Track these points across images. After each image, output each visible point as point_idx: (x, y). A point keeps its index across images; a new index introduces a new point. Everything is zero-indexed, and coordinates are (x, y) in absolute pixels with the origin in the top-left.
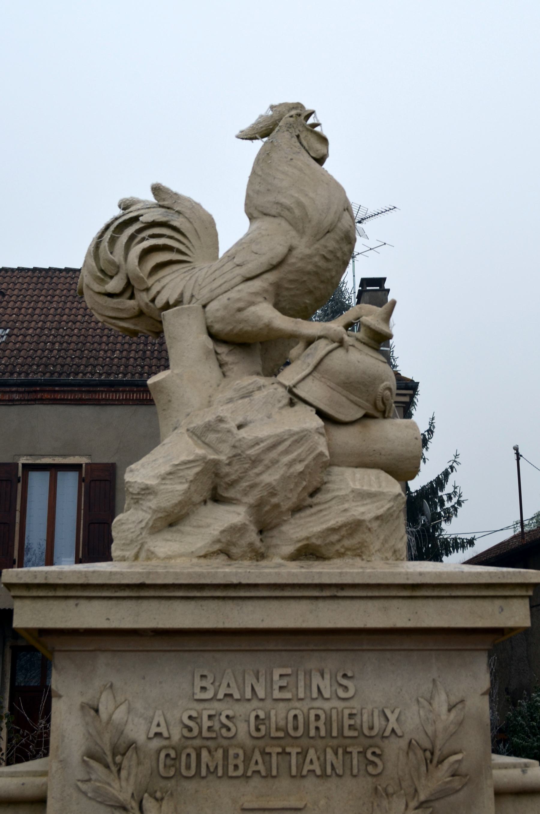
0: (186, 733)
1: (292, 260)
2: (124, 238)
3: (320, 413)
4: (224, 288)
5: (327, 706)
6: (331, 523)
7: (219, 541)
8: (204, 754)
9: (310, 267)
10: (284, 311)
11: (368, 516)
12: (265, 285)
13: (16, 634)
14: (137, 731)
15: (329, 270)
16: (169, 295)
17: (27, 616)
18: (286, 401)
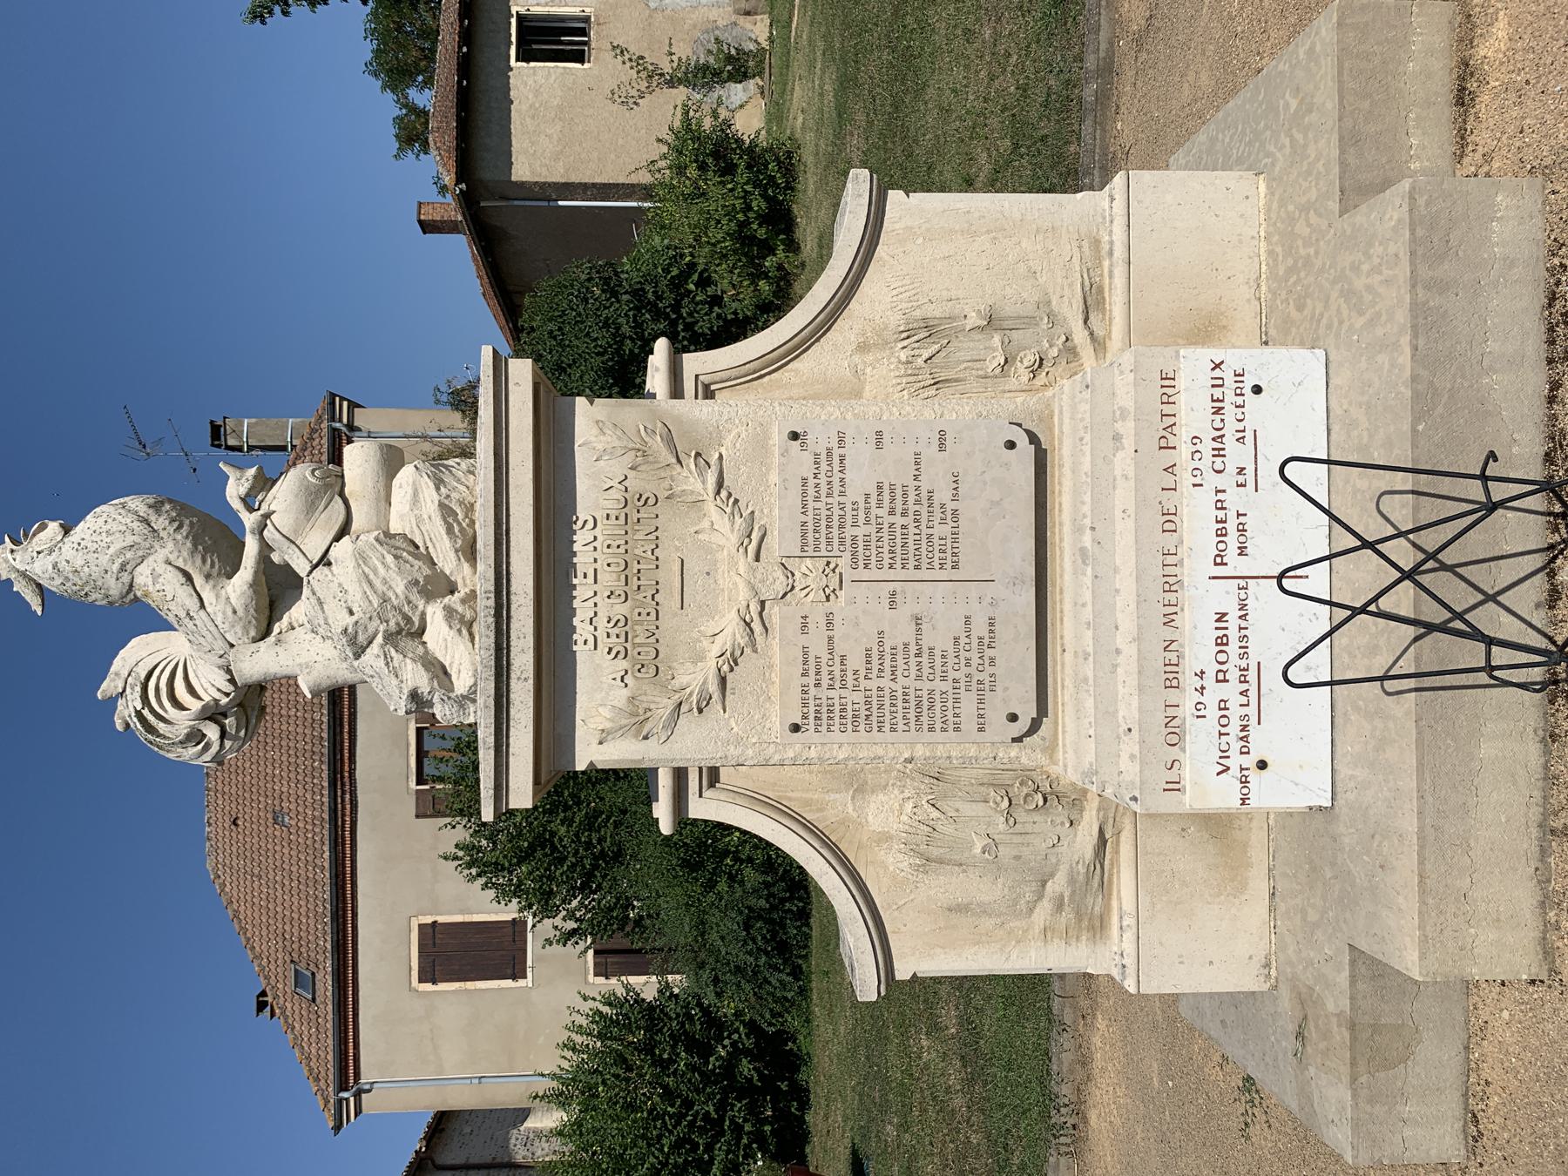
0: (622, 655)
2: (161, 727)
3: (337, 538)
4: (213, 629)
5: (600, 538)
7: (459, 631)
8: (637, 640)
9: (189, 544)
10: (236, 568)
11: (436, 497)
12: (208, 587)
14: (620, 696)
15: (192, 524)
16: (221, 681)
17: (522, 795)
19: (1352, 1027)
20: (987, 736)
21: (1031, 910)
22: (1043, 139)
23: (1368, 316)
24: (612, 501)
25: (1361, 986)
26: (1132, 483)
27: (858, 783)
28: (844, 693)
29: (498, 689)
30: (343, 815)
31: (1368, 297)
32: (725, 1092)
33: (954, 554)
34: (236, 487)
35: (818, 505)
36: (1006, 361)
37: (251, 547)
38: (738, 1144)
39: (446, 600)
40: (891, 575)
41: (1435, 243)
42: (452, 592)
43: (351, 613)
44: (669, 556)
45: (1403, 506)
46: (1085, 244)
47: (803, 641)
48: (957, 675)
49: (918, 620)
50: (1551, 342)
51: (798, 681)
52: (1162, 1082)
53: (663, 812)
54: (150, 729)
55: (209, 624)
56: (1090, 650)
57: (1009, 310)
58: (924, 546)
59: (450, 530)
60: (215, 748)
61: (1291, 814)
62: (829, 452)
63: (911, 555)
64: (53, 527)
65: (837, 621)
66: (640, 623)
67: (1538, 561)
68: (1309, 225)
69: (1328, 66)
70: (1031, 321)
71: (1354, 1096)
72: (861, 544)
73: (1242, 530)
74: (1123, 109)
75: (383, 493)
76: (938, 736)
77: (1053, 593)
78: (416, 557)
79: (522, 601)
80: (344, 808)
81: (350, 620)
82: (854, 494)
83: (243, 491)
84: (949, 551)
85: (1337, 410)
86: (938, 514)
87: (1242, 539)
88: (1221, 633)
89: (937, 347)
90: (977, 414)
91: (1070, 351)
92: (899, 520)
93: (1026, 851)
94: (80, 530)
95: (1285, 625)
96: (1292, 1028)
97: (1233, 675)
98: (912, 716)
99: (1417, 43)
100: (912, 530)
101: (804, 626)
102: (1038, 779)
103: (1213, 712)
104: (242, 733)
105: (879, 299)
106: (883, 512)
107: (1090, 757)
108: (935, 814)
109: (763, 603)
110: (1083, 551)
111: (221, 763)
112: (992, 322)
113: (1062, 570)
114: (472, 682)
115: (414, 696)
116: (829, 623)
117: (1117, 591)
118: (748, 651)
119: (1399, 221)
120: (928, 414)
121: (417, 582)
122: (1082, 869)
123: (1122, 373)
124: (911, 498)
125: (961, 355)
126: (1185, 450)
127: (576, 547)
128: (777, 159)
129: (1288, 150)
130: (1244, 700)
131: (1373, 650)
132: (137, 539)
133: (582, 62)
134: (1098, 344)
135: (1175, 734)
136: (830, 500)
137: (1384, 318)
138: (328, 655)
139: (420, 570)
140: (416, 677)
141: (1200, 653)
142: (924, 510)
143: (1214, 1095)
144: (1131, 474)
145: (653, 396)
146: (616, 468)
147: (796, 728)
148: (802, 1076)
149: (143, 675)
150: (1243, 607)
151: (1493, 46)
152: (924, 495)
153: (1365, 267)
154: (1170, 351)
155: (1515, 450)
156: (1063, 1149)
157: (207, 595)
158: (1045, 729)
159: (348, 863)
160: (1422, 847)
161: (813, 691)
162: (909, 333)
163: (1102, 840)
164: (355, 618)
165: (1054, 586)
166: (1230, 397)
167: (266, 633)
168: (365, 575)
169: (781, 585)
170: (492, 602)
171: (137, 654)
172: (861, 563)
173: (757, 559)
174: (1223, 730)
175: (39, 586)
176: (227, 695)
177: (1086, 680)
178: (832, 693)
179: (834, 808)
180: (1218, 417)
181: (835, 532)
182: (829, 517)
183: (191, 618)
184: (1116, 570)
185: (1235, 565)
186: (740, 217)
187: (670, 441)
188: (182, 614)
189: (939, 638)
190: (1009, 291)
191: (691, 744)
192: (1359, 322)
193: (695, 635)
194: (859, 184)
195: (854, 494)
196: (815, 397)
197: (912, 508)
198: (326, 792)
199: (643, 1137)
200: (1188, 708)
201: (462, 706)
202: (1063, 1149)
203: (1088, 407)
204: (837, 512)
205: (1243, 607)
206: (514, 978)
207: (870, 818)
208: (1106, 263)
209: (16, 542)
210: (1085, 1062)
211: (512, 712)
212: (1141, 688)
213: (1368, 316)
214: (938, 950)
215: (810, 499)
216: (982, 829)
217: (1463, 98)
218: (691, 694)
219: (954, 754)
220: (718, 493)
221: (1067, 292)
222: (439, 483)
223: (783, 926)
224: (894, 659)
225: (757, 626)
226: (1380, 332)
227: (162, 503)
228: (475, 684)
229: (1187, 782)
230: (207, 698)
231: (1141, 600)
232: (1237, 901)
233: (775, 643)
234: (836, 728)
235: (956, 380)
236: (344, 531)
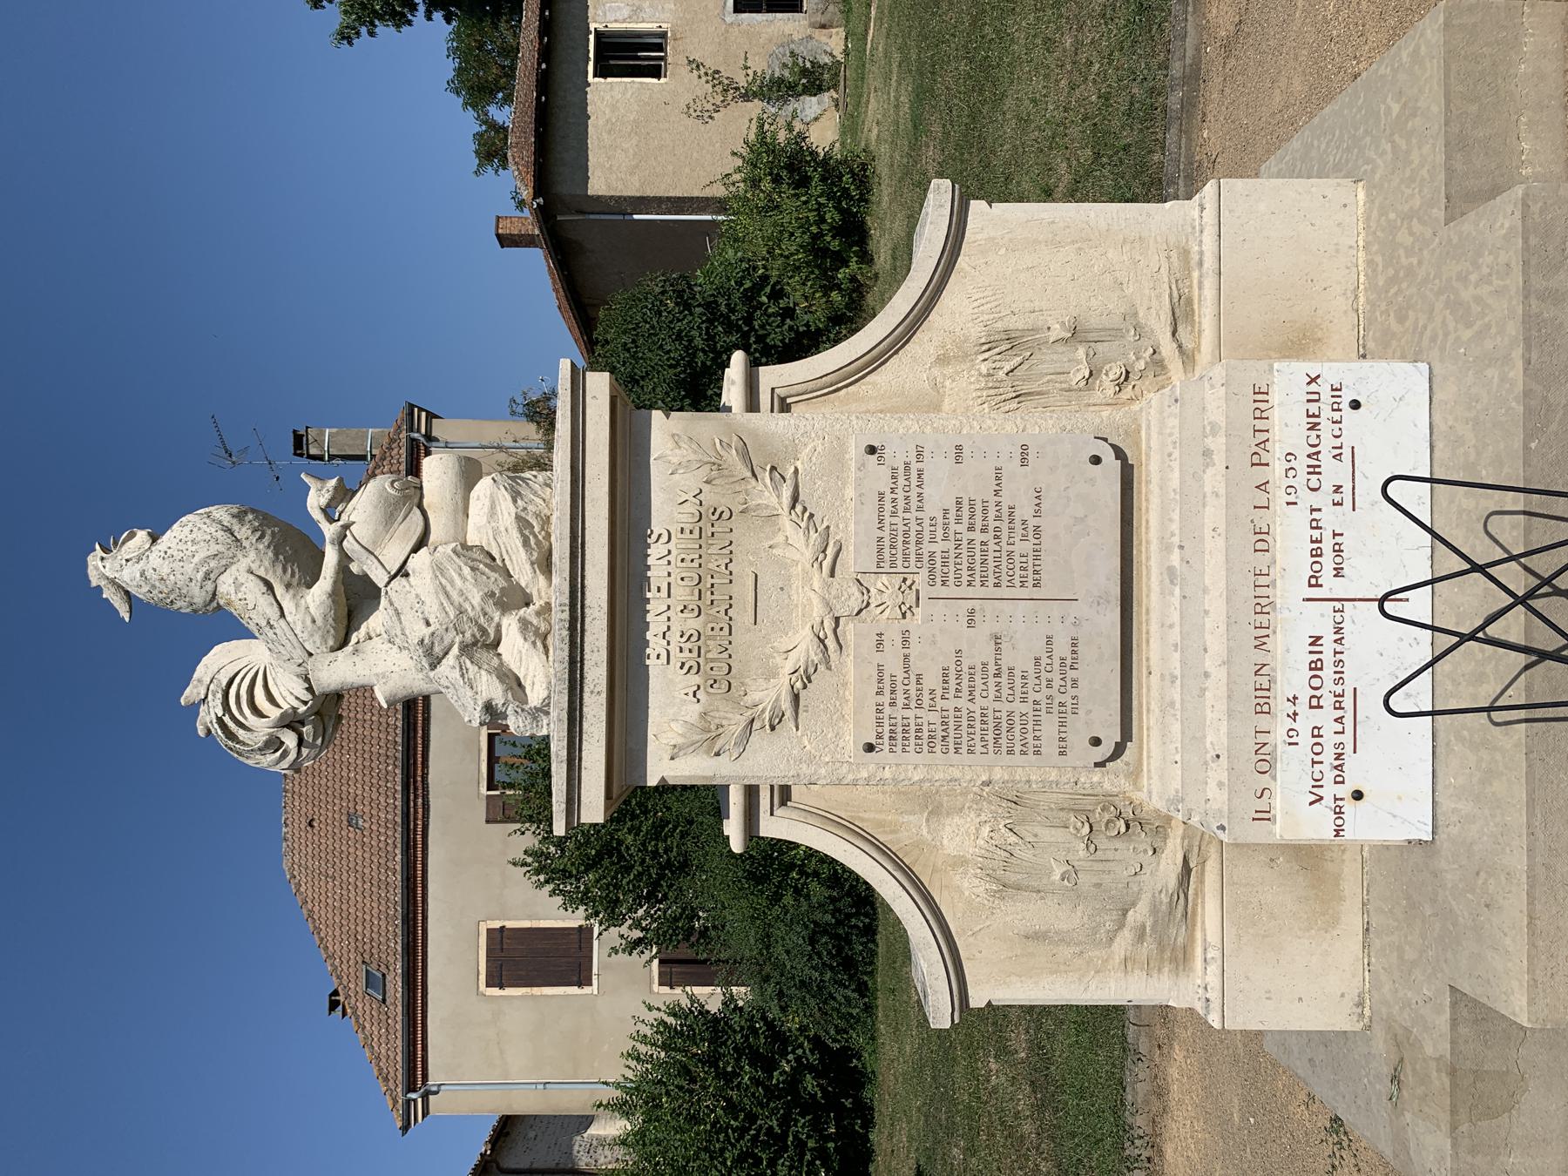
0: (695, 670)
1: (262, 573)
3: (415, 550)
4: (292, 638)
5: (674, 552)
7: (534, 643)
8: (710, 655)
9: (270, 554)
10: (315, 578)
11: (513, 510)
12: (289, 596)
13: (611, 820)
14: (692, 711)
15: (273, 533)
17: (594, 811)
18: (403, 580)
19: (1453, 1072)
22: (1126, 148)
23: (1476, 328)
25: (1463, 1030)
26: (1223, 501)
27: (933, 805)
28: (919, 712)
30: (416, 819)
31: (1476, 309)
32: (789, 1107)
33: (1036, 572)
34: (317, 498)
35: (894, 520)
36: (1091, 374)
37: (331, 558)
38: (801, 1160)
42: (527, 605)
43: (428, 624)
44: (743, 570)
45: (1513, 527)
46: (1174, 254)
48: (1038, 697)
49: (997, 639)
52: (1244, 1119)
53: (733, 830)
54: (231, 735)
55: (289, 633)
56: (1178, 672)
57: (1094, 321)
58: (1004, 563)
59: (526, 543)
60: (292, 756)
61: (1387, 847)
62: (907, 466)
63: (990, 573)
64: (142, 536)
65: (913, 639)
66: (713, 638)
68: (1411, 234)
69: (1432, 70)
70: (1116, 333)
71: (1454, 1145)
72: (939, 560)
73: (1338, 551)
74: (1210, 117)
75: (460, 505)
76: (1017, 758)
77: (1139, 614)
79: (597, 614)
80: (416, 812)
81: (427, 631)
82: (932, 509)
83: (323, 501)
84: (1031, 569)
85: (1441, 426)
87: (1338, 560)
89: (1019, 359)
91: (1157, 364)
92: (978, 536)
93: (1107, 879)
94: (167, 539)
95: (1385, 652)
96: (1386, 1071)
97: (1328, 701)
98: (990, 737)
99: (1529, 44)
100: (992, 546)
101: (880, 643)
102: (1120, 805)
103: (1305, 740)
104: (319, 741)
105: (959, 310)
106: (962, 528)
107: (1176, 784)
108: (1013, 839)
109: (837, 620)
110: (1171, 571)
111: (298, 771)
112: (1076, 334)
113: (1148, 587)
114: (545, 694)
115: (489, 707)
116: (905, 641)
117: (1206, 612)
118: (821, 668)
119: (1511, 228)
120: (1009, 428)
121: (492, 594)
122: (1166, 900)
123: (1212, 387)
124: (992, 514)
125: (1044, 368)
126: (1279, 467)
127: (650, 561)
128: (852, 171)
129: (1389, 156)
130: (1339, 728)
131: (1480, 678)
132: (220, 548)
133: (659, 77)
134: (1187, 357)
135: (1265, 762)
136: (907, 515)
137: (1493, 330)
138: (405, 666)
139: (496, 582)
140: (490, 688)
141: (1292, 678)
142: (1005, 527)
143: (1300, 1134)
144: (1222, 491)
145: (729, 409)
146: (690, 481)
147: (870, 748)
148: (867, 1094)
150: (1338, 630)
152: (1005, 511)
153: (1473, 278)
154: (1263, 364)
157: (288, 605)
158: (1128, 754)
159: (419, 866)
160: (1531, 886)
161: (887, 710)
162: (990, 345)
163: (1186, 869)
164: (431, 629)
165: (1140, 605)
166: (1327, 413)
167: (343, 643)
168: (441, 587)
169: (855, 602)
170: (566, 615)
171: (219, 661)
172: (938, 580)
173: (832, 574)
174: (1317, 758)
175: (127, 593)
176: (305, 703)
177: (1172, 704)
178: (907, 713)
179: (907, 832)
180: (1314, 433)
181: (913, 548)
182: (906, 533)
183: (272, 627)
184: (1205, 591)
185: (1331, 586)
186: (814, 229)
187: (745, 454)
188: (263, 623)
189: (1019, 658)
191: (764, 762)
192: (1467, 334)
193: (768, 650)
194: (940, 194)
195: (932, 509)
196: (893, 410)
197: (992, 524)
198: (399, 796)
199: (706, 1149)
200: (1279, 735)
201: (535, 718)
203: (1176, 422)
204: (914, 527)
205: (1338, 630)
206: (580, 985)
207: (945, 842)
208: (1196, 274)
209: (106, 550)
210: (1160, 1093)
212: (1230, 714)
213: (1476, 328)
214: (1014, 978)
215: (887, 514)
216: (1062, 856)
218: (763, 711)
219: (1033, 778)
220: (793, 507)
221: (1154, 303)
222: (516, 495)
223: (849, 942)
224: (971, 679)
226: (1489, 344)
227: (246, 513)
228: (549, 697)
229: (1278, 811)
230: (286, 706)
231: (1231, 623)
232: (1328, 936)
233: (850, 661)
234: (911, 748)
235: (1039, 393)
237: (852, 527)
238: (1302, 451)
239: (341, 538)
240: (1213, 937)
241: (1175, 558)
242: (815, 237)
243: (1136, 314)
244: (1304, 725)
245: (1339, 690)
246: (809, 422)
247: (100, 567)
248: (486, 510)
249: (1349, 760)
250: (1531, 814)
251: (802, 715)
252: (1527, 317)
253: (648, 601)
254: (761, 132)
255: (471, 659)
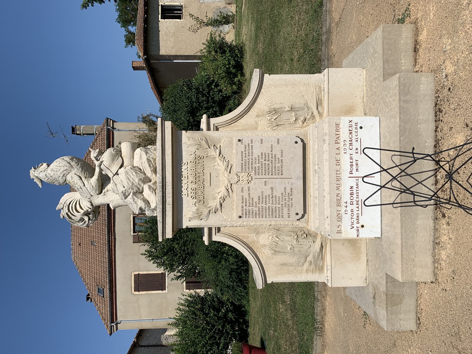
3: (120, 168)
6: (148, 166)
11: (146, 157)
12: (86, 180)
14: (194, 209)
15: (81, 164)
16: (89, 205)
17: (169, 235)
19: (386, 295)
20: (290, 219)
21: (303, 265)
22: (312, 50)
24: (192, 158)
25: (388, 284)
27: (257, 231)
29: (163, 207)
30: (112, 242)
31: (389, 104)
32: (224, 322)
33: (282, 171)
34: (93, 154)
35: (246, 158)
37: (97, 170)
39: (149, 184)
40: (265, 177)
41: (405, 91)
42: (150, 182)
43: (124, 187)
44: (207, 172)
45: (397, 159)
47: (242, 194)
48: (282, 203)
50: (436, 116)
51: (240, 205)
52: (344, 314)
53: (206, 239)
54: (70, 218)
56: (317, 196)
57: (297, 106)
59: (150, 166)
60: (87, 223)
61: (372, 239)
64: (45, 165)
65: (251, 189)
67: (432, 173)
68: (376, 83)
69: (380, 42)
70: (302, 109)
72: (257, 169)
73: (357, 165)
74: (333, 43)
76: (278, 219)
78: (141, 172)
80: (112, 240)
82: (255, 155)
83: (95, 155)
85: (382, 133)
86: (277, 161)
88: (351, 192)
89: (277, 116)
90: (287, 135)
91: (313, 116)
92: (267, 162)
93: (302, 249)
94: (52, 166)
95: (365, 190)
96: (372, 296)
97: (355, 203)
98: (271, 214)
99: (404, 35)
100: (270, 165)
102: (305, 230)
103: (349, 213)
105: (262, 103)
108: (278, 239)
109: (231, 184)
110: (315, 170)
111: (88, 227)
112: (292, 109)
115: (141, 209)
118: (228, 197)
119: (396, 84)
121: (141, 179)
122: (317, 254)
124: (270, 157)
125: (284, 118)
126: (342, 144)
127: (183, 170)
128: (238, 49)
129: (371, 63)
130: (358, 209)
131: (390, 196)
132: (67, 168)
133: (180, 19)
134: (320, 114)
135: (339, 218)
139: (142, 176)
140: (141, 204)
143: (357, 317)
144: (328, 150)
145: (202, 130)
146: (193, 149)
147: (240, 217)
149: (68, 204)
150: (357, 185)
151: (423, 37)
152: (274, 156)
153: (389, 96)
154: (338, 118)
155: (426, 144)
156: (318, 334)
157: (86, 183)
159: (113, 256)
160: (402, 247)
161: (245, 207)
163: (322, 246)
164: (125, 189)
166: (354, 130)
167: (100, 193)
168: (127, 179)
170: (161, 185)
171: (66, 198)
172: (257, 174)
173: (230, 173)
175: (41, 180)
176: (90, 209)
177: (316, 204)
178: (249, 208)
179: (251, 238)
181: (250, 165)
184: (324, 175)
185: (355, 174)
186: (227, 66)
187: (207, 142)
188: (79, 188)
189: (278, 193)
190: (297, 101)
191: (213, 221)
192: (387, 110)
193: (214, 193)
194: (256, 73)
195: (255, 155)
196: (245, 130)
197: (270, 159)
198: (106, 236)
199: (201, 335)
200: (343, 211)
201: (153, 212)
202: (318, 334)
203: (316, 132)
204: (251, 160)
205: (357, 185)
206: (162, 290)
208: (323, 93)
209: (35, 169)
210: (324, 310)
211: (167, 213)
212: (330, 206)
214: (278, 275)
215: (244, 157)
217: (416, 50)
221: (312, 101)
222: (147, 153)
223: (241, 274)
224: (266, 199)
225: (230, 190)
226: (392, 113)
229: (343, 231)
230: (85, 210)
231: (330, 183)
233: (235, 195)
234: (251, 217)
236: (122, 166)
237: (235, 160)
238: (348, 140)
239: (100, 165)
240: (329, 263)
241: (316, 167)
242: (228, 69)
243: (307, 104)
244: (349, 209)
245: (357, 200)
246: (224, 134)
247: (33, 173)
248: (139, 157)
249: (360, 218)
250: (402, 230)
251: (223, 209)
252: (400, 107)
253: (182, 180)
254: (211, 37)
255: (136, 196)
